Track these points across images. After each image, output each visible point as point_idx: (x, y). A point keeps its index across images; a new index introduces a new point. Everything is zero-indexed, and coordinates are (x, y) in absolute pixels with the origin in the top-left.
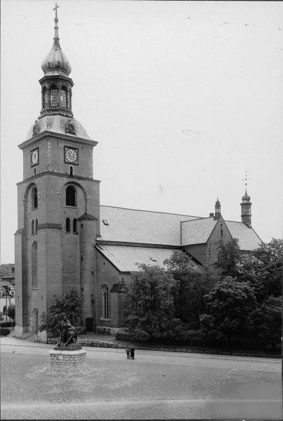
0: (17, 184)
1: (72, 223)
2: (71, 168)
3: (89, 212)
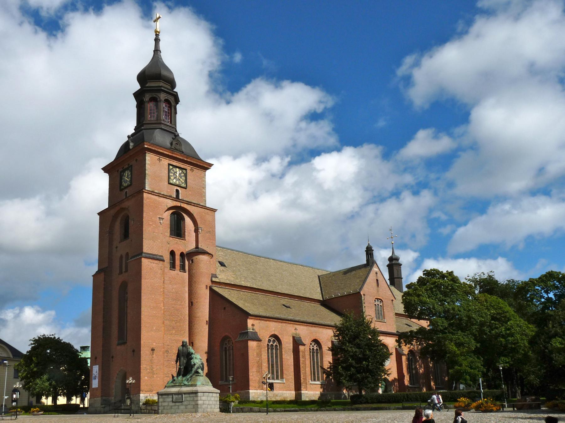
1: (178, 257)
2: (177, 191)
3: (202, 246)
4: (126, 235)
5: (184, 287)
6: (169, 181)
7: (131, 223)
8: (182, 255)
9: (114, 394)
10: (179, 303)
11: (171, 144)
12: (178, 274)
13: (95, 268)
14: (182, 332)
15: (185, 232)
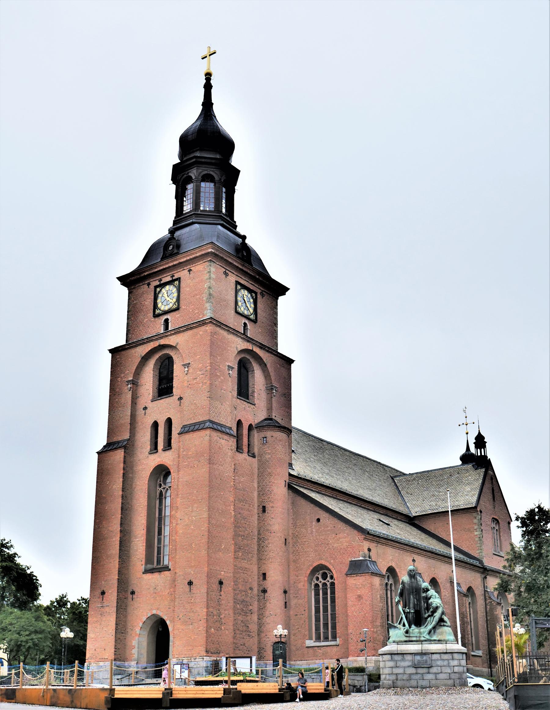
0: (111, 351)
1: (245, 431)
5: (253, 482)
9: (136, 656)
10: (247, 506)
12: (245, 459)
14: (250, 555)
15: (254, 392)
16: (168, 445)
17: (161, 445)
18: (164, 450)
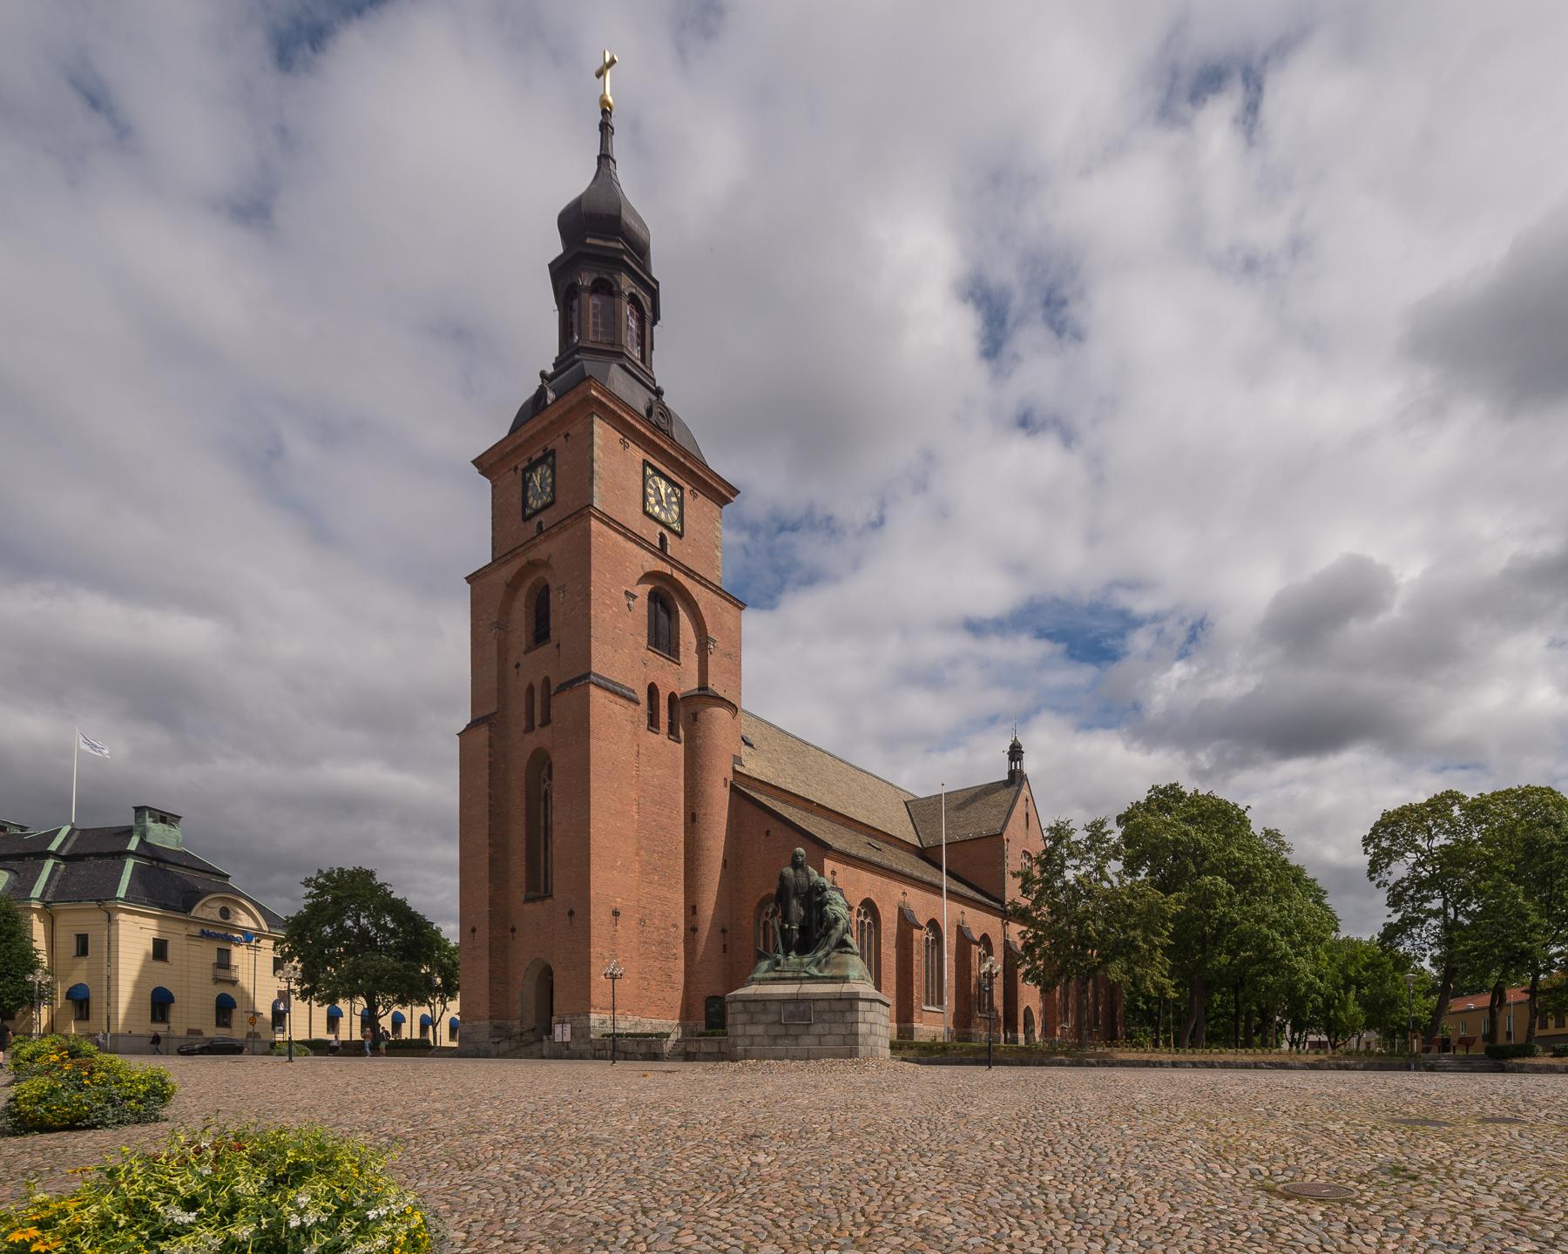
2: (663, 539)
4: (541, 632)
6: (644, 506)
7: (555, 598)
8: (672, 697)
11: (649, 411)
13: (464, 718)
16: (546, 721)
17: (538, 721)
18: (543, 725)
